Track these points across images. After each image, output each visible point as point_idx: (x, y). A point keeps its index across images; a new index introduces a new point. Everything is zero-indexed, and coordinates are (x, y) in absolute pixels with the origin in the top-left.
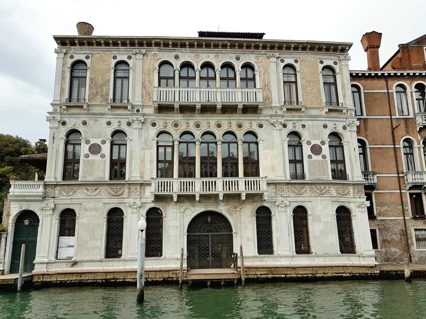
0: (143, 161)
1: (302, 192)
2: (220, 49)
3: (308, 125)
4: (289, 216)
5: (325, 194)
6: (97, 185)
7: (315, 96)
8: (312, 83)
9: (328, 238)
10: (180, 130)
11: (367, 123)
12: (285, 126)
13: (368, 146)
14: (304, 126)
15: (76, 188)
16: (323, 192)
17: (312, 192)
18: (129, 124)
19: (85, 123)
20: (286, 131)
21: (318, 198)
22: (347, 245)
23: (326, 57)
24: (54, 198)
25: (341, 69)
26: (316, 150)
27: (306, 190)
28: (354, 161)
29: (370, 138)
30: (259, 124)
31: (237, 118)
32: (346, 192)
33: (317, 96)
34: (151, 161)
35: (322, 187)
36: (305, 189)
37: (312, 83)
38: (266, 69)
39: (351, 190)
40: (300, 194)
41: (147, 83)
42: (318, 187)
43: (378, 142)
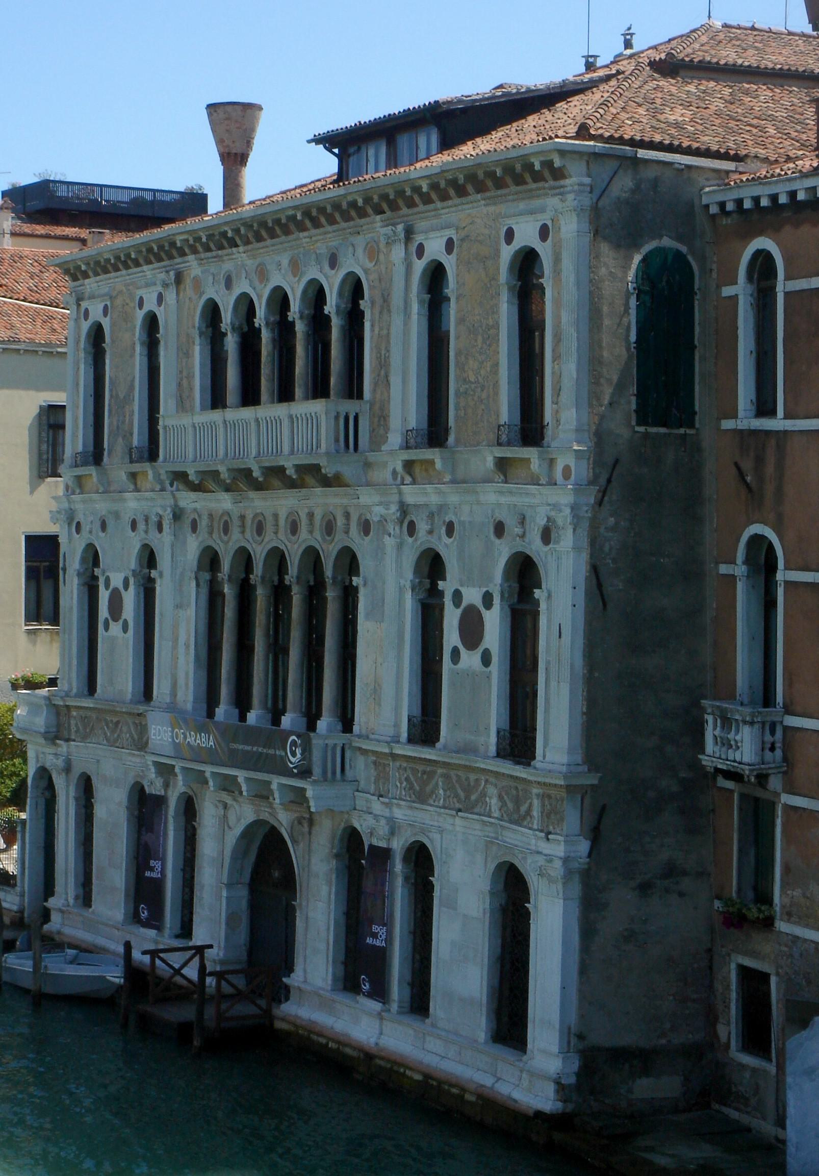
3: (459, 521)
5: (473, 808)
7: (484, 395)
8: (480, 338)
12: (412, 529)
13: (780, 576)
16: (473, 797)
17: (448, 793)
18: (160, 528)
19: (104, 526)
21: (458, 821)
22: (509, 1022)
23: (522, 206)
25: (557, 259)
28: (553, 684)
32: (523, 808)
33: (488, 397)
34: (187, 646)
35: (472, 777)
36: (434, 782)
37: (480, 338)
40: (422, 798)
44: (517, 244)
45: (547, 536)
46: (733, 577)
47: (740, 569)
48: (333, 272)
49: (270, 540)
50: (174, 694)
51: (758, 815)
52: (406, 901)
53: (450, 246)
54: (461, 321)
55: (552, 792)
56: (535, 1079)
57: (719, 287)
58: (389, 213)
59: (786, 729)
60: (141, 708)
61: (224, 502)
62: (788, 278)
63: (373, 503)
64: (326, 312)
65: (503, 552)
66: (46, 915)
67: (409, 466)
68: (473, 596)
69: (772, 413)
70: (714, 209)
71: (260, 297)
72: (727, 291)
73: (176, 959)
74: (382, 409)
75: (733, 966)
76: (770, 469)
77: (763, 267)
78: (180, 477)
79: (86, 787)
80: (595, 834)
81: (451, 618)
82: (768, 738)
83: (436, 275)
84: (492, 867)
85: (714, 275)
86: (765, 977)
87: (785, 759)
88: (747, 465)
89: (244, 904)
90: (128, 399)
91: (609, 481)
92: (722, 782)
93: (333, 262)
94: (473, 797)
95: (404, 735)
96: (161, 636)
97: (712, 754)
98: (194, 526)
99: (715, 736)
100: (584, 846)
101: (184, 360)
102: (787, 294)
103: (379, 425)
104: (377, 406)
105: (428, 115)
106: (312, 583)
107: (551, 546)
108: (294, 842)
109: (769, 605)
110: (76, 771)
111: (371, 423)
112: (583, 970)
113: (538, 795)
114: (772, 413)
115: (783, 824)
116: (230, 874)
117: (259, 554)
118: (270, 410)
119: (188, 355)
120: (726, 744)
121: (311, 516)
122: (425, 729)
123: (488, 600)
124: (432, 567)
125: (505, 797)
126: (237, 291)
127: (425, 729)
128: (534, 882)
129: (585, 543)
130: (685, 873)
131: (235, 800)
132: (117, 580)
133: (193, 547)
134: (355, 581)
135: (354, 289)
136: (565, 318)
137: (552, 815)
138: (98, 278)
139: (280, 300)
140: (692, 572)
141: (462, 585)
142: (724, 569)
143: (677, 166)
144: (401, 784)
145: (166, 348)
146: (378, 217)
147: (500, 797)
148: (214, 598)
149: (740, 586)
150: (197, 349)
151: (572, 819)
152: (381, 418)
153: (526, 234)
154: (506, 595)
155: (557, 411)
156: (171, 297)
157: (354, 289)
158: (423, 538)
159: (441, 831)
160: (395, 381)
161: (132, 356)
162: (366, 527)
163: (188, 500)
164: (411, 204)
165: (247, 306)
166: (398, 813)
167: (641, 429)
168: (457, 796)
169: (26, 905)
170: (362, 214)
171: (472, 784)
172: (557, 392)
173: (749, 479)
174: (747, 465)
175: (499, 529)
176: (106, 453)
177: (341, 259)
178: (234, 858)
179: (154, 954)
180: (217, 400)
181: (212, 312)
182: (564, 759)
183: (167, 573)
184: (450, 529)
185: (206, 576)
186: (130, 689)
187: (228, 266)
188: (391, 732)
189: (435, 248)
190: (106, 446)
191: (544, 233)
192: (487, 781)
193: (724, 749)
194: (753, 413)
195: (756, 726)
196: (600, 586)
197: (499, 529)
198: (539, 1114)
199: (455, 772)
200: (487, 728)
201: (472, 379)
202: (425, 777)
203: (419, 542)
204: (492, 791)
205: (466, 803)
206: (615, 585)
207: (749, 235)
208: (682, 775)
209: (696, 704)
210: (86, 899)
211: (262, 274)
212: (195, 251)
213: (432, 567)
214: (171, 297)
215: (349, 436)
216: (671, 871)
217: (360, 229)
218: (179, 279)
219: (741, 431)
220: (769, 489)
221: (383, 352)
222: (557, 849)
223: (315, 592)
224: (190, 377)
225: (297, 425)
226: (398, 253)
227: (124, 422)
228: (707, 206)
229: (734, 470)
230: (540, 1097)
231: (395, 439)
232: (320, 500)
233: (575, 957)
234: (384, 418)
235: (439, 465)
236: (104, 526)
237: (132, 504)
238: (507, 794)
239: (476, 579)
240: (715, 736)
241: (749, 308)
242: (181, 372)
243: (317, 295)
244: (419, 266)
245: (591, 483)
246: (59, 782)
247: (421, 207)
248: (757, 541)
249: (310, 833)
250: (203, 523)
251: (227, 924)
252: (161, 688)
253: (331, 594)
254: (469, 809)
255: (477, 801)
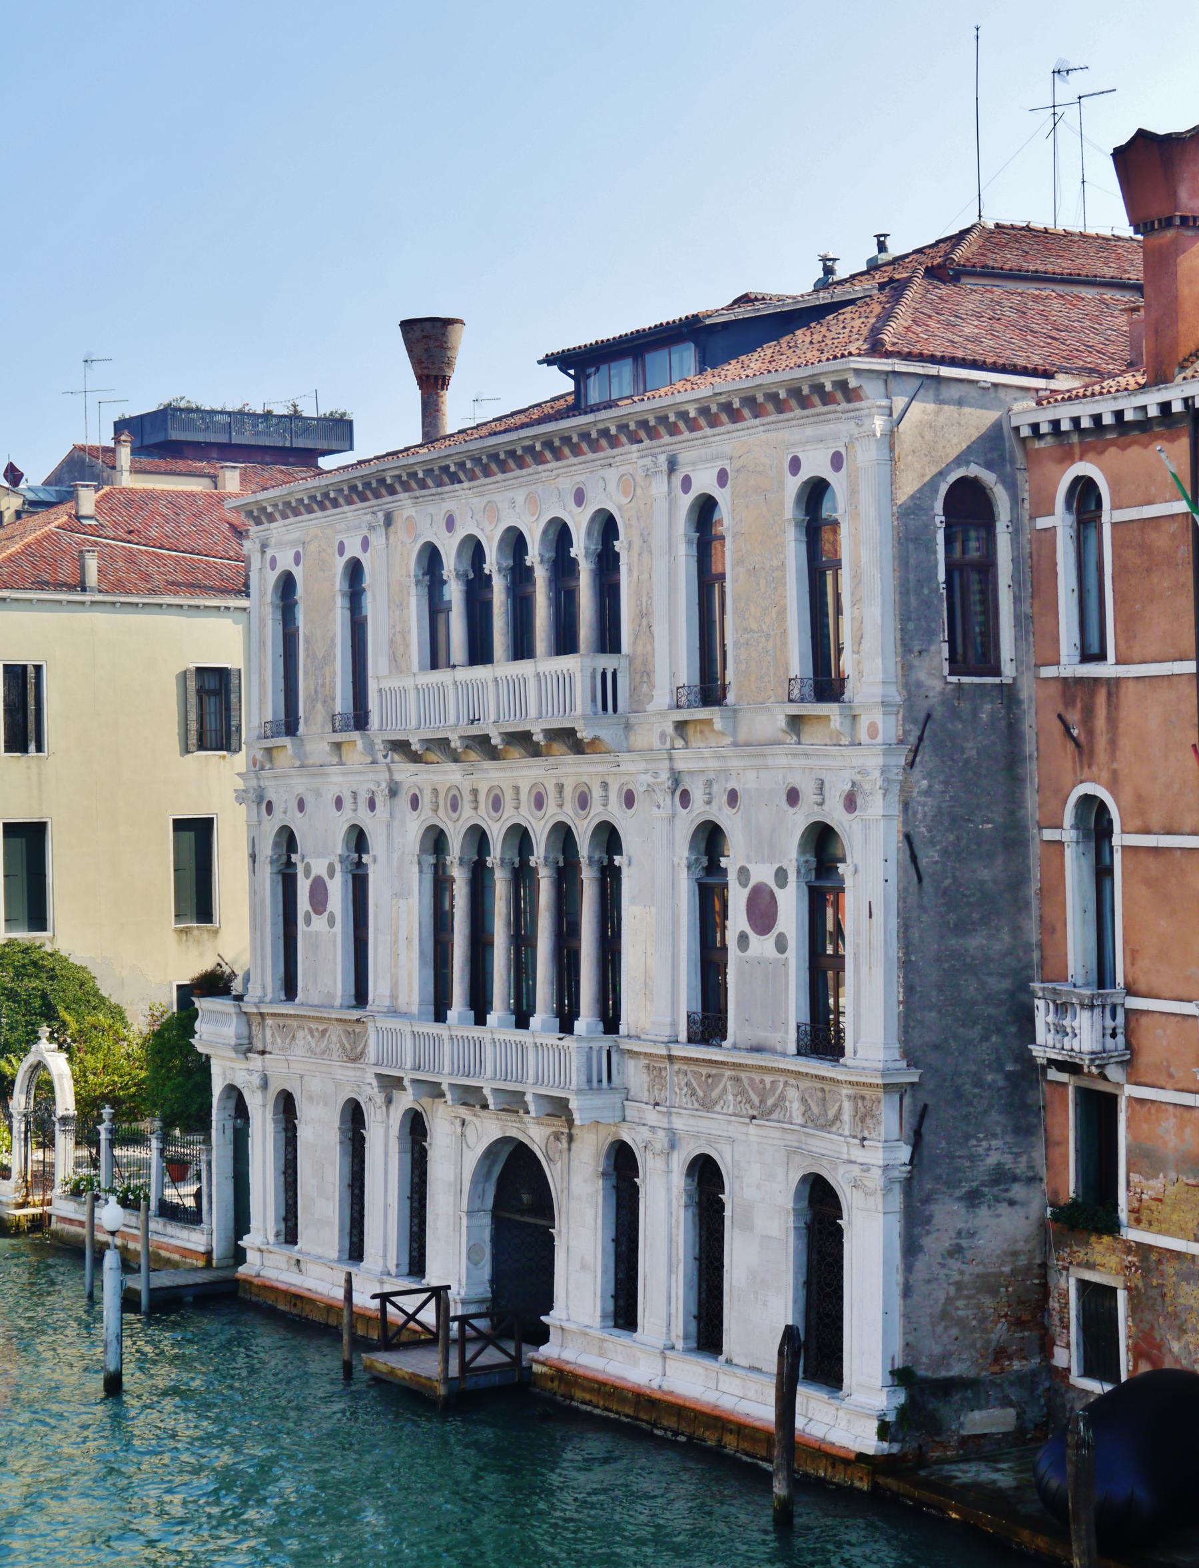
0: (396, 941)
1: (715, 1094)
2: (530, 470)
4: (675, 1192)
5: (770, 1113)
6: (318, 1021)
7: (770, 646)
8: (763, 582)
9: (765, 1304)
10: (460, 822)
11: (1117, 708)
12: (685, 798)
13: (1117, 840)
14: (733, 798)
15: (295, 1024)
16: (770, 1102)
17: (739, 1098)
18: (372, 805)
19: (301, 805)
20: (687, 823)
21: (752, 1130)
23: (809, 431)
24: (263, 1053)
25: (853, 491)
26: (762, 912)
27: (725, 1090)
28: (864, 970)
29: (1127, 795)
30: (625, 789)
31: (572, 770)
32: (831, 1113)
34: (409, 940)
35: (768, 1079)
36: (721, 1086)
37: (763, 582)
38: (645, 533)
39: (847, 1106)
40: (707, 1105)
41: (398, 639)
42: (757, 1078)
43: (1156, 818)
44: (805, 474)
45: (850, 803)
46: (1060, 843)
47: (1068, 834)
48: (580, 509)
49: (511, 816)
50: (394, 996)
51: (1099, 1111)
52: (690, 1225)
53: (722, 478)
54: (739, 562)
55: (867, 1092)
56: (849, 1419)
57: (1032, 518)
58: (647, 443)
59: (1128, 1012)
60: (355, 1014)
61: (450, 775)
62: (1114, 507)
63: (634, 771)
64: (572, 555)
65: (798, 822)
66: (239, 1256)
67: (681, 726)
68: (763, 874)
69: (1101, 657)
70: (1025, 432)
71: (489, 539)
72: (1042, 523)
73: (410, 1303)
74: (645, 663)
75: (1072, 1281)
76: (1100, 723)
77: (1084, 496)
78: (401, 747)
79: (287, 1106)
80: (917, 1140)
81: (737, 898)
82: (1109, 1023)
83: (706, 508)
84: (796, 1177)
85: (1027, 505)
86: (1114, 1290)
87: (1129, 1046)
88: (1074, 717)
89: (487, 1234)
90: (328, 659)
91: (921, 739)
92: (1053, 1075)
93: (579, 498)
94: (770, 1102)
95: (683, 1036)
96: (376, 929)
97: (1045, 1045)
98: (415, 803)
99: (1048, 1024)
100: (904, 1153)
101: (397, 613)
102: (1115, 525)
103: (641, 682)
104: (638, 662)
105: (684, 330)
106: (561, 864)
107: (856, 813)
108: (549, 1159)
109: (1103, 873)
110: (274, 1088)
111: (632, 680)
112: (907, 1292)
113: (849, 1097)
114: (1101, 657)
115: (1128, 1119)
116: (470, 1199)
117: (496, 833)
118: (503, 668)
119: (402, 606)
120: (1061, 1031)
121: (560, 788)
122: (709, 1023)
123: (781, 876)
124: (710, 839)
125: (809, 1101)
126: (460, 534)
127: (709, 1023)
128: (849, 1198)
129: (896, 809)
130: (1015, 1179)
131: (475, 1115)
132: (319, 868)
133: (413, 829)
134: (617, 860)
135: (607, 527)
136: (865, 555)
137: (864, 1116)
138: (287, 521)
139: (516, 542)
140: (1013, 839)
141: (749, 862)
142: (1048, 835)
143: (982, 384)
144: (681, 1089)
145: (374, 599)
146: (635, 447)
147: (803, 1100)
148: (441, 884)
149: (1069, 853)
150: (413, 601)
151: (889, 1119)
152: (645, 673)
153: (816, 465)
154: (803, 871)
155: (859, 662)
156: (377, 540)
157: (607, 527)
158: (699, 811)
159: (732, 1141)
160: (660, 630)
161: (332, 609)
162: (629, 800)
163: (405, 772)
164: (673, 430)
165: (475, 550)
166: (678, 1123)
167: (953, 679)
168: (749, 1101)
169: (214, 1245)
170: (614, 442)
171: (768, 1086)
172: (859, 640)
173: (1075, 732)
174: (1074, 717)
175: (793, 797)
176: (302, 721)
177: (589, 495)
178: (475, 1182)
179: (384, 1298)
180: (436, 658)
181: (431, 558)
182: (881, 1055)
183: (382, 858)
184: (733, 798)
185: (432, 860)
186: (339, 993)
187: (448, 505)
188: (667, 1031)
189: (705, 482)
190: (301, 713)
191: (837, 461)
192: (786, 1083)
193: (1059, 1037)
194: (1078, 659)
195: (1097, 1011)
196: (914, 858)
197: (793, 797)
198: (861, 1457)
199: (748, 1074)
200: (786, 1023)
201: (754, 626)
202: (710, 1081)
203: (694, 814)
204: (792, 1094)
205: (762, 1110)
206: (929, 857)
207: (1068, 458)
208: (1009, 1068)
209: (1023, 987)
210: (290, 1235)
211: (492, 511)
212: (407, 488)
213: (710, 839)
214: (377, 540)
215: (606, 694)
216: (1002, 1177)
217: (611, 460)
218: (389, 521)
219: (1065, 679)
220: (1102, 742)
221: (644, 599)
222: (874, 1156)
223: (566, 877)
224: (404, 634)
225: (545, 685)
226: (659, 486)
227: (323, 686)
228: (1017, 429)
229: (1057, 724)
230: (861, 1437)
231: (662, 698)
232: (569, 769)
233: (898, 1278)
234: (648, 675)
235: (718, 725)
236: (301, 805)
237: (337, 782)
238: (811, 1096)
239: (763, 855)
240: (1048, 1024)
241: (1069, 541)
242: (394, 627)
243: (560, 535)
244: (686, 501)
245: (901, 742)
246: (254, 1102)
247: (687, 435)
248: (1088, 800)
249: (569, 1149)
250: (426, 800)
251: (469, 1258)
252: (377, 988)
253: (588, 877)
254: (766, 1114)
255: (775, 1106)
